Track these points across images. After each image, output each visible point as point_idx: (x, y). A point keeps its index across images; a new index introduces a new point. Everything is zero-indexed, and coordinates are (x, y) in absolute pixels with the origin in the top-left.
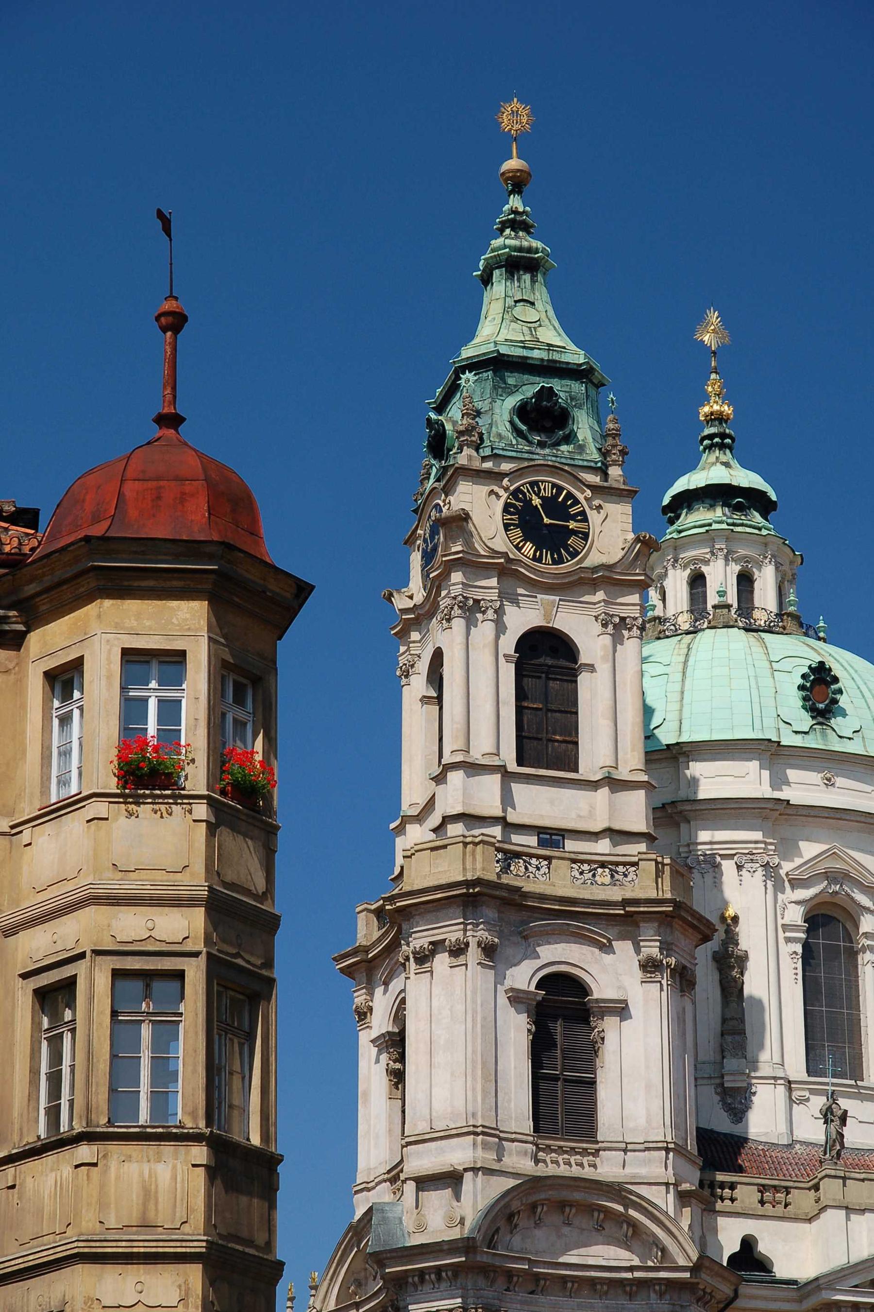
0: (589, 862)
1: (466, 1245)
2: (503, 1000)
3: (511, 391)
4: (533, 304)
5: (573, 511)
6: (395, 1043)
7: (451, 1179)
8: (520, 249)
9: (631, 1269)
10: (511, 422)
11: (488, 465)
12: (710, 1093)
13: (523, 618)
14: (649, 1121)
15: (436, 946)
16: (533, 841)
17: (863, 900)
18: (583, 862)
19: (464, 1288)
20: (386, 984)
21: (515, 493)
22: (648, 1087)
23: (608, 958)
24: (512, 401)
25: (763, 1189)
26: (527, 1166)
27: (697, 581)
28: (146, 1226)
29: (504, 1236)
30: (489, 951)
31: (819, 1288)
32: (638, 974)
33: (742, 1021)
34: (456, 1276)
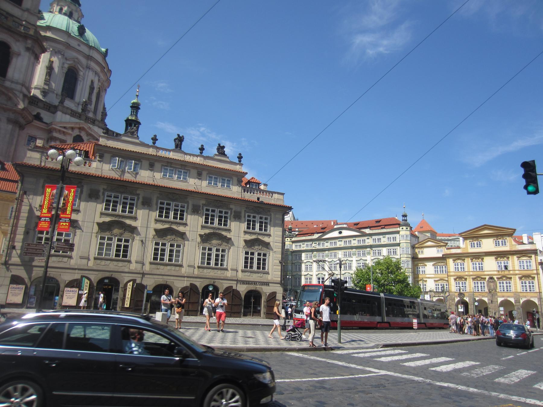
0: (18, 23)
17: (81, 69)
23: (18, 44)
27: (61, 10)
31: (52, 124)
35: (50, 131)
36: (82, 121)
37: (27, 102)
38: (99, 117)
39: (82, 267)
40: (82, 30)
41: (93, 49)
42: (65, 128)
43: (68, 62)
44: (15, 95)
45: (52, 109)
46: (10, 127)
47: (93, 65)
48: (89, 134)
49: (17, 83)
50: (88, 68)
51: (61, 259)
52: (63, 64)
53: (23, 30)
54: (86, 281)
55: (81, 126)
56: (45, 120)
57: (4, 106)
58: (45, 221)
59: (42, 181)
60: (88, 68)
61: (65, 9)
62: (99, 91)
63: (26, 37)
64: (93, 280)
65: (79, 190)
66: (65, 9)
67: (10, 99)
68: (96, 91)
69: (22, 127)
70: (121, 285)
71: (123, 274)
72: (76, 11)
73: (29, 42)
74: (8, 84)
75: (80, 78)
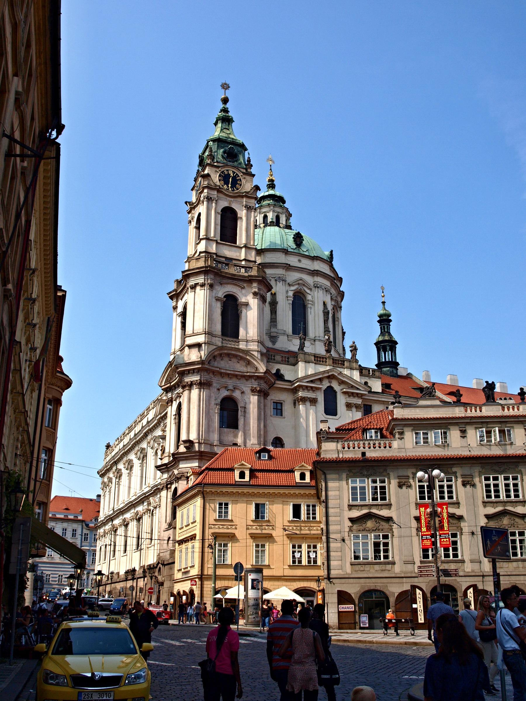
0: (239, 266)
1: (202, 362)
2: (214, 300)
4: (228, 129)
5: (238, 178)
6: (184, 315)
7: (198, 346)
8: (226, 116)
9: (247, 372)
11: (215, 164)
13: (224, 203)
15: (196, 285)
16: (224, 259)
17: (308, 291)
18: (238, 266)
19: (200, 375)
20: (181, 299)
21: (223, 172)
22: (253, 325)
23: (244, 291)
24: (222, 150)
26: (220, 344)
27: (265, 217)
29: (212, 363)
30: (211, 286)
33: (276, 319)
34: (198, 372)
35: (295, 391)
37: (265, 361)
38: (348, 355)
39: (409, 575)
40: (298, 238)
41: (317, 259)
42: (312, 381)
44: (252, 356)
45: (291, 359)
50: (316, 287)
51: (383, 567)
52: (287, 292)
53: (246, 272)
54: (418, 591)
55: (330, 374)
56: (286, 378)
57: (245, 374)
58: (427, 539)
61: (271, 216)
62: (334, 312)
63: (250, 280)
64: (424, 589)
66: (271, 216)
67: (249, 363)
68: (330, 315)
70: (460, 594)
71: (458, 579)
73: (255, 285)
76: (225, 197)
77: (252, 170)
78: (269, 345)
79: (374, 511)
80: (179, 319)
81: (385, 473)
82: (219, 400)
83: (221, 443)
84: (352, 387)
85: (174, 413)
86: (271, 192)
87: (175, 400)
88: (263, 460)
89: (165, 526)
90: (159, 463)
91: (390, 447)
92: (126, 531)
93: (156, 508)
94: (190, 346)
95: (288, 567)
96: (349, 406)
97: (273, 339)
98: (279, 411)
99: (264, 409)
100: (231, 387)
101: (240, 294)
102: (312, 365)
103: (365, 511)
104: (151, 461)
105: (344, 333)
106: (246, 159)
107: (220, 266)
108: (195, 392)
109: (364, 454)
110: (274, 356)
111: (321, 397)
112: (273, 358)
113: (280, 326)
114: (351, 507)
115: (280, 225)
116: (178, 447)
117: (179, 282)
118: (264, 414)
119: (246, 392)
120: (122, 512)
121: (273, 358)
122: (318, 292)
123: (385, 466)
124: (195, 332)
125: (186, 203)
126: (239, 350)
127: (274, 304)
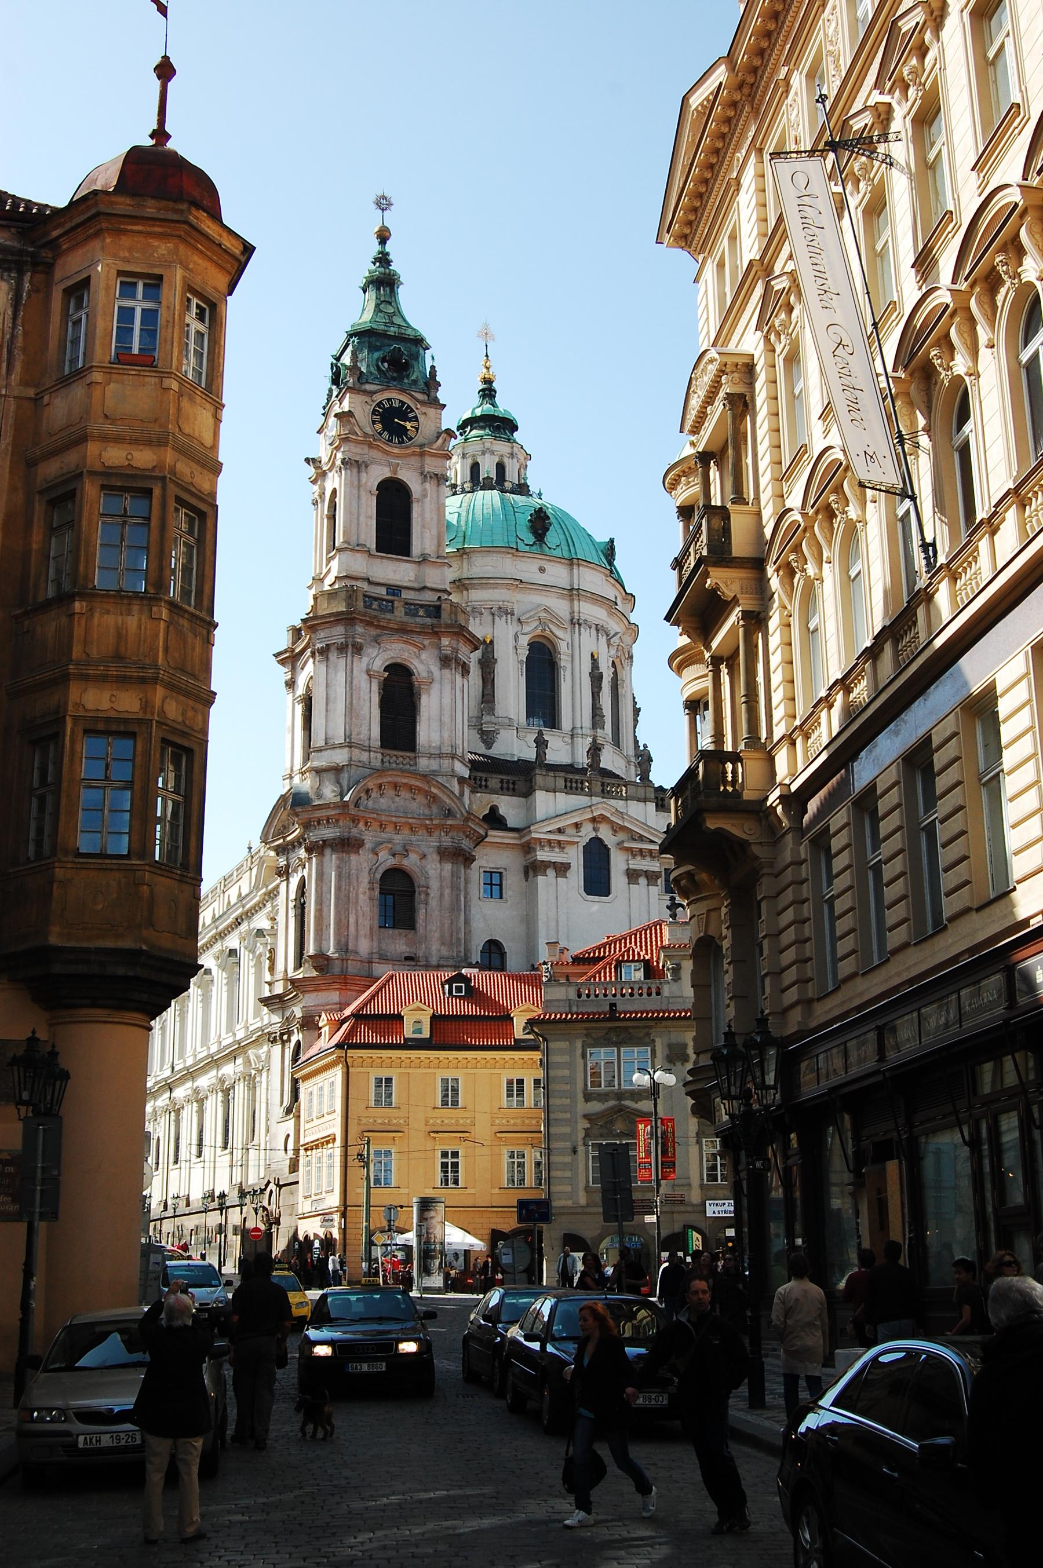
2: (366, 677)
3: (378, 349)
4: (390, 303)
7: (337, 770)
8: (385, 274)
10: (377, 366)
12: (475, 735)
14: (442, 743)
22: (442, 724)
25: (502, 781)
26: (376, 763)
27: (475, 468)
28: (118, 657)
29: (364, 801)
31: (530, 832)
32: (438, 664)
35: (527, 848)
36: (595, 800)
42: (560, 831)
43: (527, 629)
44: (442, 787)
46: (448, 867)
47: (588, 610)
48: (616, 829)
49: (440, 756)
54: (695, 1235)
56: (510, 823)
59: (579, 1044)
60: (575, 623)
61: (488, 469)
62: (615, 673)
65: (649, 1049)
67: (435, 798)
69: (468, 860)
72: (512, 455)
73: (445, 641)
74: (424, 764)
75: (564, 661)
76: (386, 457)
77: (438, 395)
78: (482, 749)
79: (627, 1103)
80: (299, 709)
81: (647, 1040)
82: (378, 876)
83: (384, 958)
84: (641, 839)
85: (292, 896)
86: (487, 408)
87: (295, 871)
88: (456, 997)
89: (278, 1112)
90: (267, 994)
91: (658, 994)
92: (201, 1112)
93: (260, 1071)
94: (318, 771)
95: (497, 1191)
96: (633, 876)
97: (488, 738)
98: (496, 889)
99: (466, 888)
100: (399, 848)
101: (416, 662)
102: (561, 796)
103: (612, 1103)
104: (251, 985)
105: (637, 711)
106: (428, 370)
107: (375, 605)
108: (332, 859)
109: (613, 1005)
110: (486, 780)
111: (575, 857)
112: (484, 783)
113: (499, 710)
114: (588, 1097)
115: (506, 484)
116: (298, 965)
117: (296, 633)
118: (465, 898)
119: (429, 857)
120: (190, 1074)
121: (484, 783)
122: (580, 634)
123: (647, 1027)
124: (331, 742)
125: (307, 460)
126: (416, 774)
127: (488, 665)
